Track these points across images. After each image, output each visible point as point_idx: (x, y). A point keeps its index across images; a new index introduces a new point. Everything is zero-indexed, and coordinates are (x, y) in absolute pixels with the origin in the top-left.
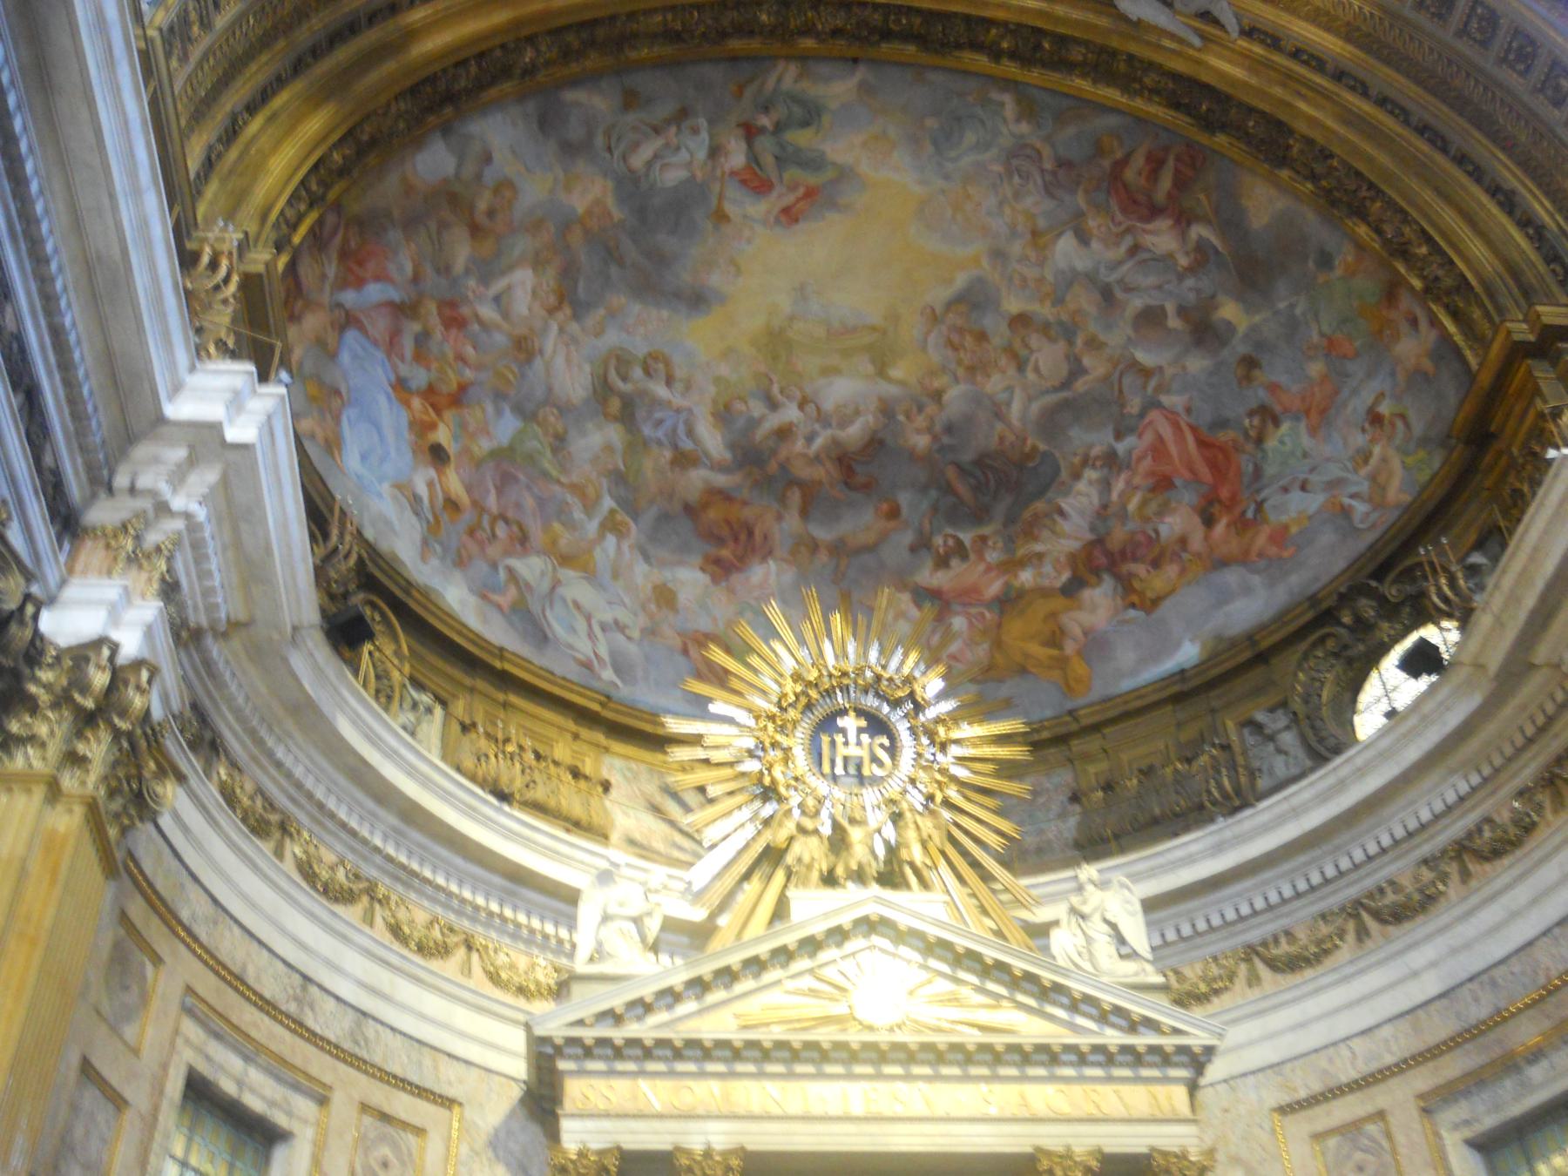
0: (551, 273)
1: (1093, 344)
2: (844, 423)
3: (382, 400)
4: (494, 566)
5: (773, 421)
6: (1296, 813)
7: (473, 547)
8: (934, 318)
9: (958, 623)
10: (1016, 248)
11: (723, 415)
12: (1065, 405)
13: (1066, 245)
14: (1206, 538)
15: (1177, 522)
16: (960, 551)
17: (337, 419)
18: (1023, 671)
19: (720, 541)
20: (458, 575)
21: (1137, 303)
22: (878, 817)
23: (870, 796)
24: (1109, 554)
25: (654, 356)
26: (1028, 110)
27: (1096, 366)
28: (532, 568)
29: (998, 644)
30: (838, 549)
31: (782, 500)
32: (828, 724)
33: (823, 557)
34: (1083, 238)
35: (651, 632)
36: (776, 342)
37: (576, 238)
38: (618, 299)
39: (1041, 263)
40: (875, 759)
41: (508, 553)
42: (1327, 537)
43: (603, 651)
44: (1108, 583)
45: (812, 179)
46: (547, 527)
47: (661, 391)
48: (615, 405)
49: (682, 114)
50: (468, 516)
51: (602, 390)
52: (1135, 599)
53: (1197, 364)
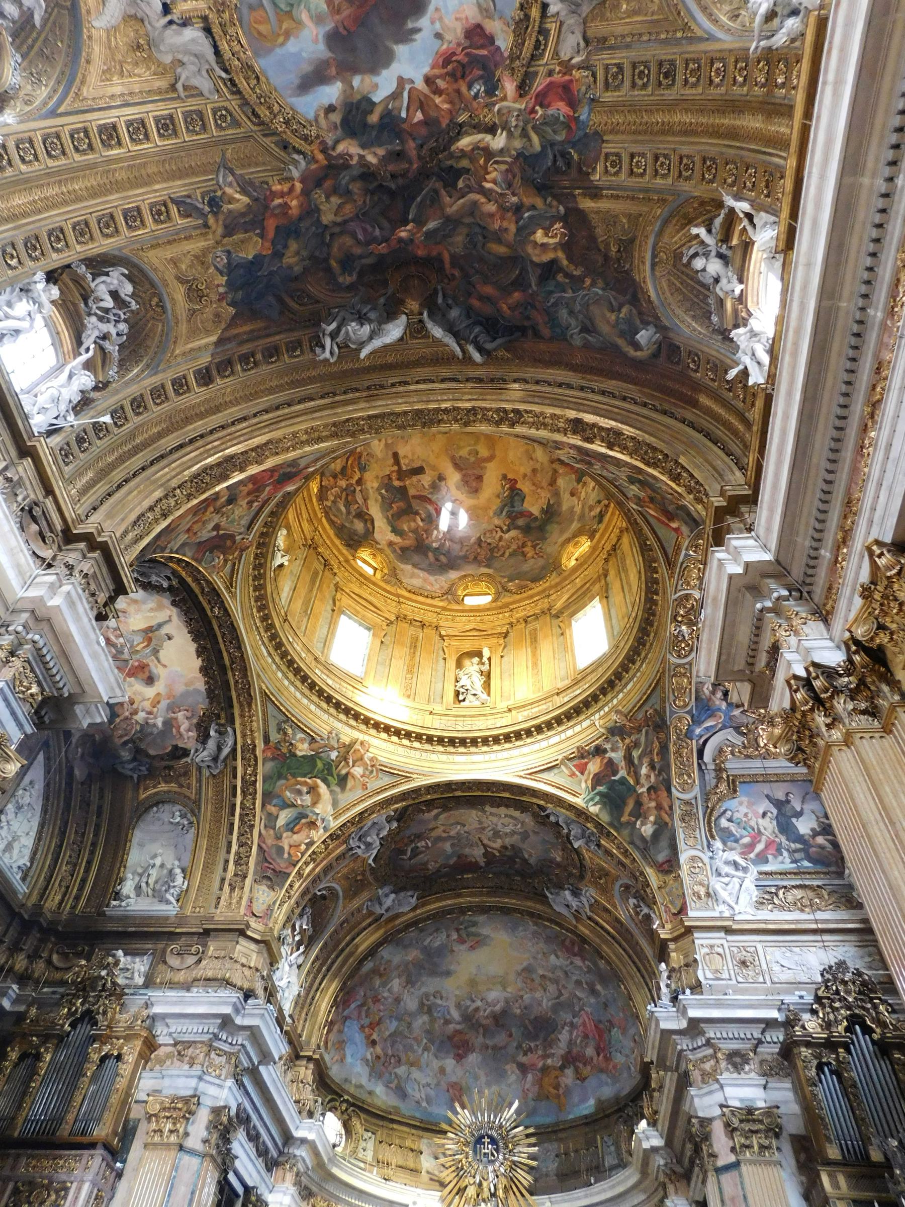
0: (404, 978)
1: (564, 986)
5: (474, 1006)
8: (519, 974)
9: (530, 1077)
10: (540, 956)
11: (458, 1006)
12: (559, 1004)
13: (553, 957)
15: (590, 1051)
16: (530, 1050)
19: (458, 1048)
21: (574, 978)
22: (491, 1176)
23: (490, 1168)
25: (437, 992)
26: (536, 924)
28: (401, 1070)
29: (541, 1087)
30: (494, 1048)
32: (479, 1140)
33: (490, 1051)
34: (557, 957)
35: (438, 1084)
36: (473, 983)
37: (411, 966)
38: (424, 979)
40: (493, 1155)
42: (625, 1075)
44: (572, 1068)
45: (477, 939)
47: (439, 1002)
49: (437, 930)
50: (382, 1059)
51: (422, 1004)
53: (593, 1000)
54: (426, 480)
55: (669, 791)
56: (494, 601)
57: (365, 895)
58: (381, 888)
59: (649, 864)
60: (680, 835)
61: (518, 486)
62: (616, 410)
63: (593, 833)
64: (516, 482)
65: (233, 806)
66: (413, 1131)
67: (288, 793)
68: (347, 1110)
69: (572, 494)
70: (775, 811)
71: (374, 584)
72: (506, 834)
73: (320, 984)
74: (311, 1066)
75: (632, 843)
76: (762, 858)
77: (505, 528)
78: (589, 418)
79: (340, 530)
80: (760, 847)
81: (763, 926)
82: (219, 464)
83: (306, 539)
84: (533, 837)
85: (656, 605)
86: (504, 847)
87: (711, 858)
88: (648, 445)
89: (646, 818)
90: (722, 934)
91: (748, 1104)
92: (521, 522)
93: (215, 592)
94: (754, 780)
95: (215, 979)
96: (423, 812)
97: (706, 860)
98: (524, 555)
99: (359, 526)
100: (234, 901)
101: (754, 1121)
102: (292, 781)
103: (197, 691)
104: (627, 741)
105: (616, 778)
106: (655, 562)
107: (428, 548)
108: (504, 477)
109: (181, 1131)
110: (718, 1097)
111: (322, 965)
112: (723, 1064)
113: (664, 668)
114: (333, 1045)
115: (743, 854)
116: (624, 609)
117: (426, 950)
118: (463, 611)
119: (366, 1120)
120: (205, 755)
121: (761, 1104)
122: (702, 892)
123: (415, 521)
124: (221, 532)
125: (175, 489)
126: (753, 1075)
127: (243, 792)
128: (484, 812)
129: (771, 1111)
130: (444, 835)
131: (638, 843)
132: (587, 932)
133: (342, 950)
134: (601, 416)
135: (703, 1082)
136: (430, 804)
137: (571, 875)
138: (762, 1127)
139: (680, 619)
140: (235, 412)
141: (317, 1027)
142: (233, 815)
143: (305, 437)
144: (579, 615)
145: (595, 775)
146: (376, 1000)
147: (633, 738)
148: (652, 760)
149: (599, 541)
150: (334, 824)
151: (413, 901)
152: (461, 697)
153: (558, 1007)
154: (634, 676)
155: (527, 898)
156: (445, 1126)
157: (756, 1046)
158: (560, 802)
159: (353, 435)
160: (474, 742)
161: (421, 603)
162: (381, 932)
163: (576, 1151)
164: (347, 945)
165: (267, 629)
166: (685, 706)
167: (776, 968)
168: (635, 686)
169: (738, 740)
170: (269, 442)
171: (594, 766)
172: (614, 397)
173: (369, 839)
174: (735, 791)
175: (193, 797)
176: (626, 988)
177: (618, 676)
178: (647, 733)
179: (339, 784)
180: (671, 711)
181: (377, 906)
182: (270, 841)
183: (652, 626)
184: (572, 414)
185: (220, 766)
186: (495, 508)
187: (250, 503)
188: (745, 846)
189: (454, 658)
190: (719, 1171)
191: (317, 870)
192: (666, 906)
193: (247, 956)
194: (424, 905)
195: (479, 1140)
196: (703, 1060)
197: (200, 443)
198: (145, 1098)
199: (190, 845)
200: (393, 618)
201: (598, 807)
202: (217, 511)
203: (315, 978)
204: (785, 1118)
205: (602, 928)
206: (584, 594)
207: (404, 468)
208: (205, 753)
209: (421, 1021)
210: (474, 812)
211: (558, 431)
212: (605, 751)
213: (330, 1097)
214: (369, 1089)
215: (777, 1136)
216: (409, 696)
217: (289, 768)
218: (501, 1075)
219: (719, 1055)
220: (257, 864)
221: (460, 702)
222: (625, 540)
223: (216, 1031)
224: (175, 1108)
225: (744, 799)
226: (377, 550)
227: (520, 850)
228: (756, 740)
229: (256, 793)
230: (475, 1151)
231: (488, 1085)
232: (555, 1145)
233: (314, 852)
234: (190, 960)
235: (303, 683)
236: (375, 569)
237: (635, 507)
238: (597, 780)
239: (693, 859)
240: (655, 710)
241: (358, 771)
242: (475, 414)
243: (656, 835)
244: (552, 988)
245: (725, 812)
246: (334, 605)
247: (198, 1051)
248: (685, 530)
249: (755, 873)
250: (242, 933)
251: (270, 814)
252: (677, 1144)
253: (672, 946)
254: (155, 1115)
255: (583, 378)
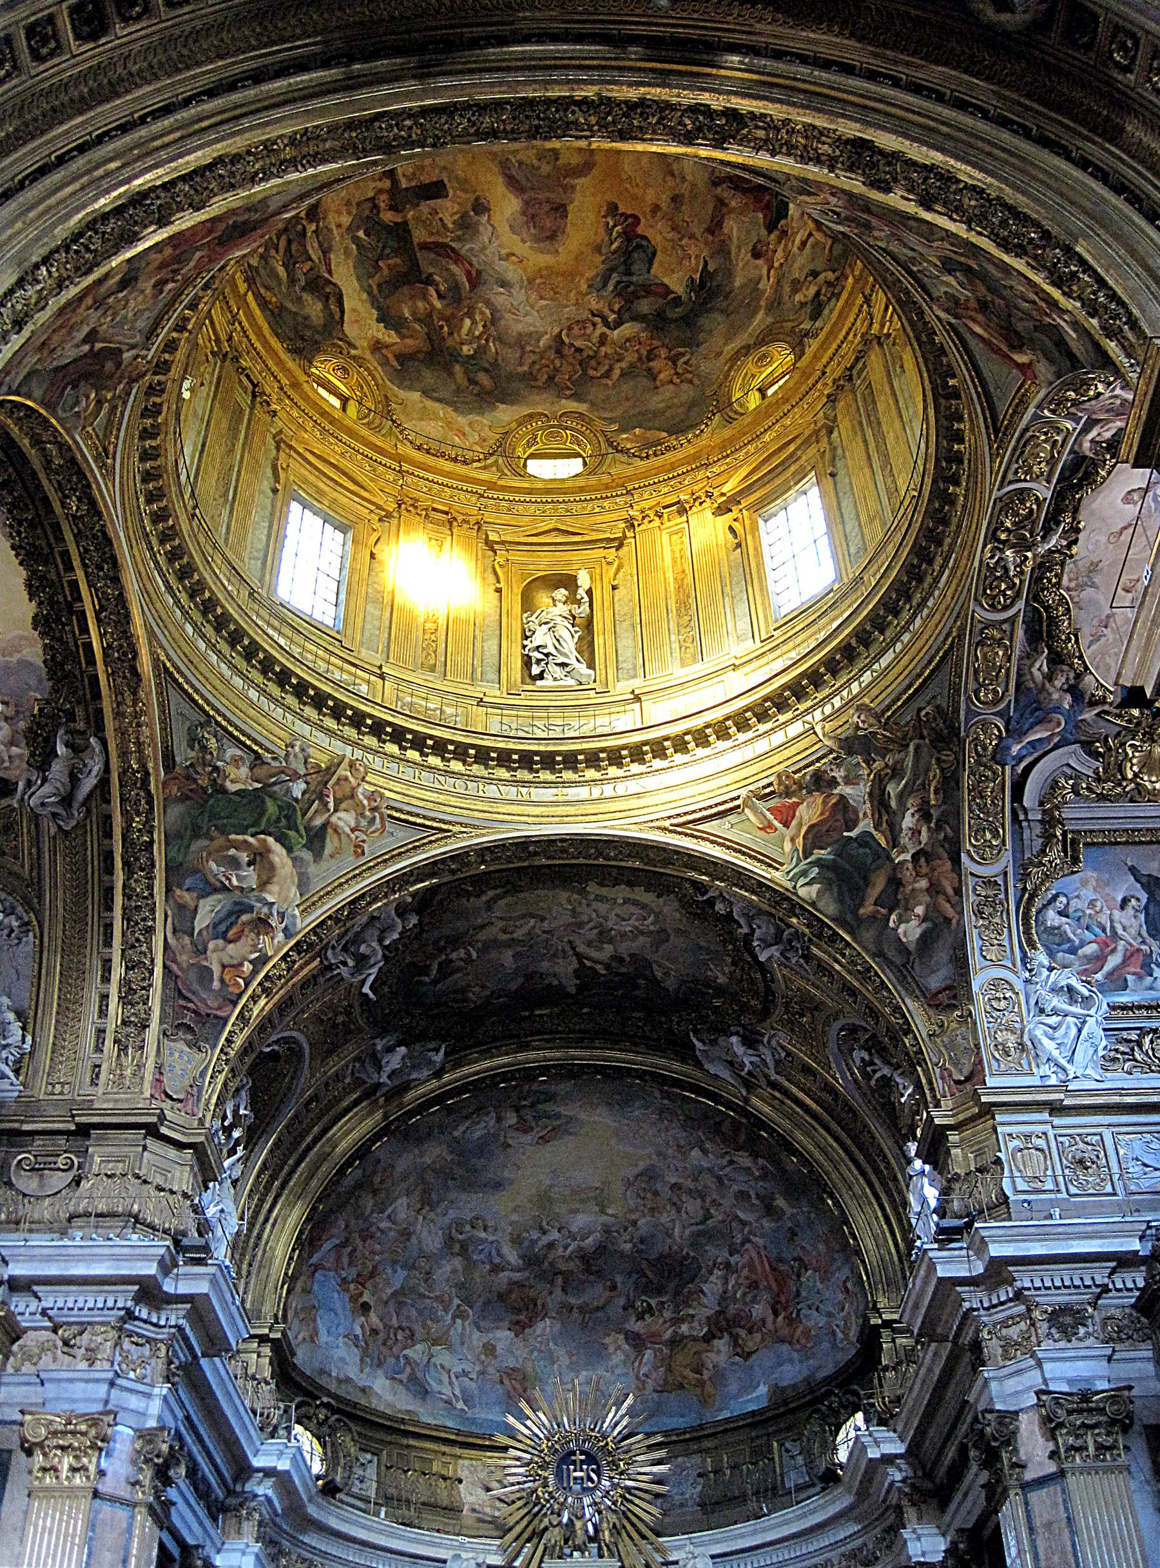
2: (582, 1240)
3: (336, 1295)
4: (398, 1358)
5: (545, 1240)
6: (787, 1522)
7: (385, 1350)
8: (629, 1184)
9: (648, 1355)
11: (516, 1241)
13: (696, 1153)
14: (774, 1322)
15: (759, 1310)
16: (649, 1310)
17: (314, 1321)
18: (681, 1387)
19: (519, 1311)
20: (380, 1372)
21: (735, 1188)
23: (587, 1501)
24: (728, 1321)
26: (667, 1095)
27: (718, 1215)
28: (416, 1352)
29: (670, 1370)
31: (552, 1283)
32: (567, 1458)
33: (575, 1314)
34: (705, 1152)
35: (482, 1373)
36: (543, 1200)
37: (429, 1177)
38: (452, 1195)
39: (684, 1161)
40: (590, 1479)
41: (405, 1348)
42: (826, 1345)
43: (457, 1392)
46: (424, 1325)
47: (483, 1235)
48: (457, 1248)
50: (382, 1336)
51: (449, 1241)
52: (739, 1350)
53: (767, 1224)
54: (448, 209)
55: (956, 861)
56: (590, 469)
57: (350, 1051)
58: (381, 1035)
59: (911, 993)
60: (974, 942)
61: (640, 230)
62: (945, 129)
63: (797, 935)
64: (637, 220)
65: (109, 891)
66: (444, 1449)
67: (213, 865)
68: (327, 1418)
69: (756, 255)
70: (1144, 897)
71: (351, 433)
72: (623, 935)
73: (270, 1211)
74: (267, 1350)
75: (879, 954)
76: (1116, 981)
77: (612, 317)
78: (888, 141)
79: (276, 315)
80: (1113, 961)
81: (1116, 1099)
82: (118, 211)
83: (218, 341)
84: (676, 941)
85: (953, 503)
86: (620, 960)
87: (1026, 981)
88: (1012, 209)
89: (908, 909)
90: (1045, 1116)
91: (1083, 1386)
92: (645, 306)
93: (74, 467)
94: (1111, 841)
95: (113, 1215)
96: (468, 894)
97: (1019, 985)
98: (652, 375)
99: (314, 308)
100: (128, 1072)
101: (1090, 1410)
102: (220, 841)
103: (25, 664)
104: (878, 765)
105: (852, 834)
106: (960, 419)
107: (455, 356)
108: (613, 209)
109: (92, 1468)
110: (1033, 1379)
111: (273, 1178)
112: (1043, 1327)
113: (962, 629)
114: (296, 1314)
115: (1085, 975)
116: (872, 504)
117: (460, 1149)
118: (530, 491)
119: (360, 1434)
120: (45, 794)
121: (1102, 1385)
122: (1011, 1041)
123: (425, 297)
124: (99, 345)
125: (37, 266)
126: (1090, 1342)
127: (126, 863)
128: (582, 892)
129: (1120, 1394)
130: (505, 937)
131: (891, 954)
132: (767, 1109)
133: (309, 1148)
134: (914, 139)
135: (1006, 1357)
136: (481, 882)
137: (745, 1008)
138: (1103, 1419)
139: (1003, 537)
140: (146, 95)
141: (271, 1285)
142: (110, 909)
143: (288, 153)
144: (773, 507)
145: (811, 827)
146: (366, 1235)
147: (890, 759)
148: (925, 802)
149: (816, 357)
150: (304, 924)
151: (438, 1058)
152: (536, 670)
153: (703, 1236)
154: (897, 638)
155: (656, 1048)
156: (504, 1440)
157: (1099, 1296)
158: (739, 877)
159: (387, 148)
160: (571, 761)
161: (447, 475)
162: (379, 1115)
163: (734, 1467)
164: (315, 1141)
165: (164, 538)
166: (995, 702)
167: (1135, 1169)
168: (898, 658)
169: (1087, 766)
170: (219, 161)
171: (809, 812)
172: (940, 98)
173: (363, 949)
174: (1075, 860)
175: (26, 875)
176: (837, 1203)
177: (863, 637)
178: (918, 748)
179: (308, 846)
180: (969, 711)
181: (371, 1070)
182: (183, 958)
183: (940, 544)
184: (850, 129)
185: (78, 814)
186: (590, 274)
187: (159, 285)
188: (1089, 959)
189: (518, 590)
190: (1026, 1487)
191: (270, 1005)
192: (943, 1068)
193: (164, 1172)
194: (458, 1065)
195: (567, 1458)
196: (1005, 1324)
197: (80, 163)
198: (18, 1417)
199: (28, 968)
200: (391, 506)
201: (816, 887)
202: (98, 304)
203: (262, 1201)
204: (1138, 1403)
205: (797, 1101)
206: (784, 465)
207: (404, 184)
208: (47, 789)
209: (448, 1268)
210: (564, 895)
211: (818, 161)
212: (833, 782)
213: (298, 1400)
214: (361, 1384)
215: (1125, 1430)
216: (433, 669)
217: (213, 816)
218: (597, 1354)
219: (1036, 1314)
220: (164, 1002)
221: (534, 678)
222: (875, 359)
223: (130, 1304)
224: (73, 1433)
225: (1091, 874)
226: (350, 363)
227: (649, 964)
228: (1121, 769)
229: (153, 865)
230: (559, 1475)
231: (573, 1367)
232: (696, 1459)
233: (267, 977)
234: (58, 1180)
235: (233, 647)
236: (345, 401)
237: (943, 315)
238: (815, 837)
239: (996, 984)
240: (938, 707)
241: (345, 819)
242: (644, 116)
243: (926, 940)
244: (693, 1207)
245: (1055, 898)
246: (277, 480)
247: (99, 1339)
248: (1044, 370)
249: (1105, 1006)
250: (152, 1131)
251: (181, 907)
252: (928, 1447)
253: (953, 1137)
254: (41, 1445)
255: (875, 55)
